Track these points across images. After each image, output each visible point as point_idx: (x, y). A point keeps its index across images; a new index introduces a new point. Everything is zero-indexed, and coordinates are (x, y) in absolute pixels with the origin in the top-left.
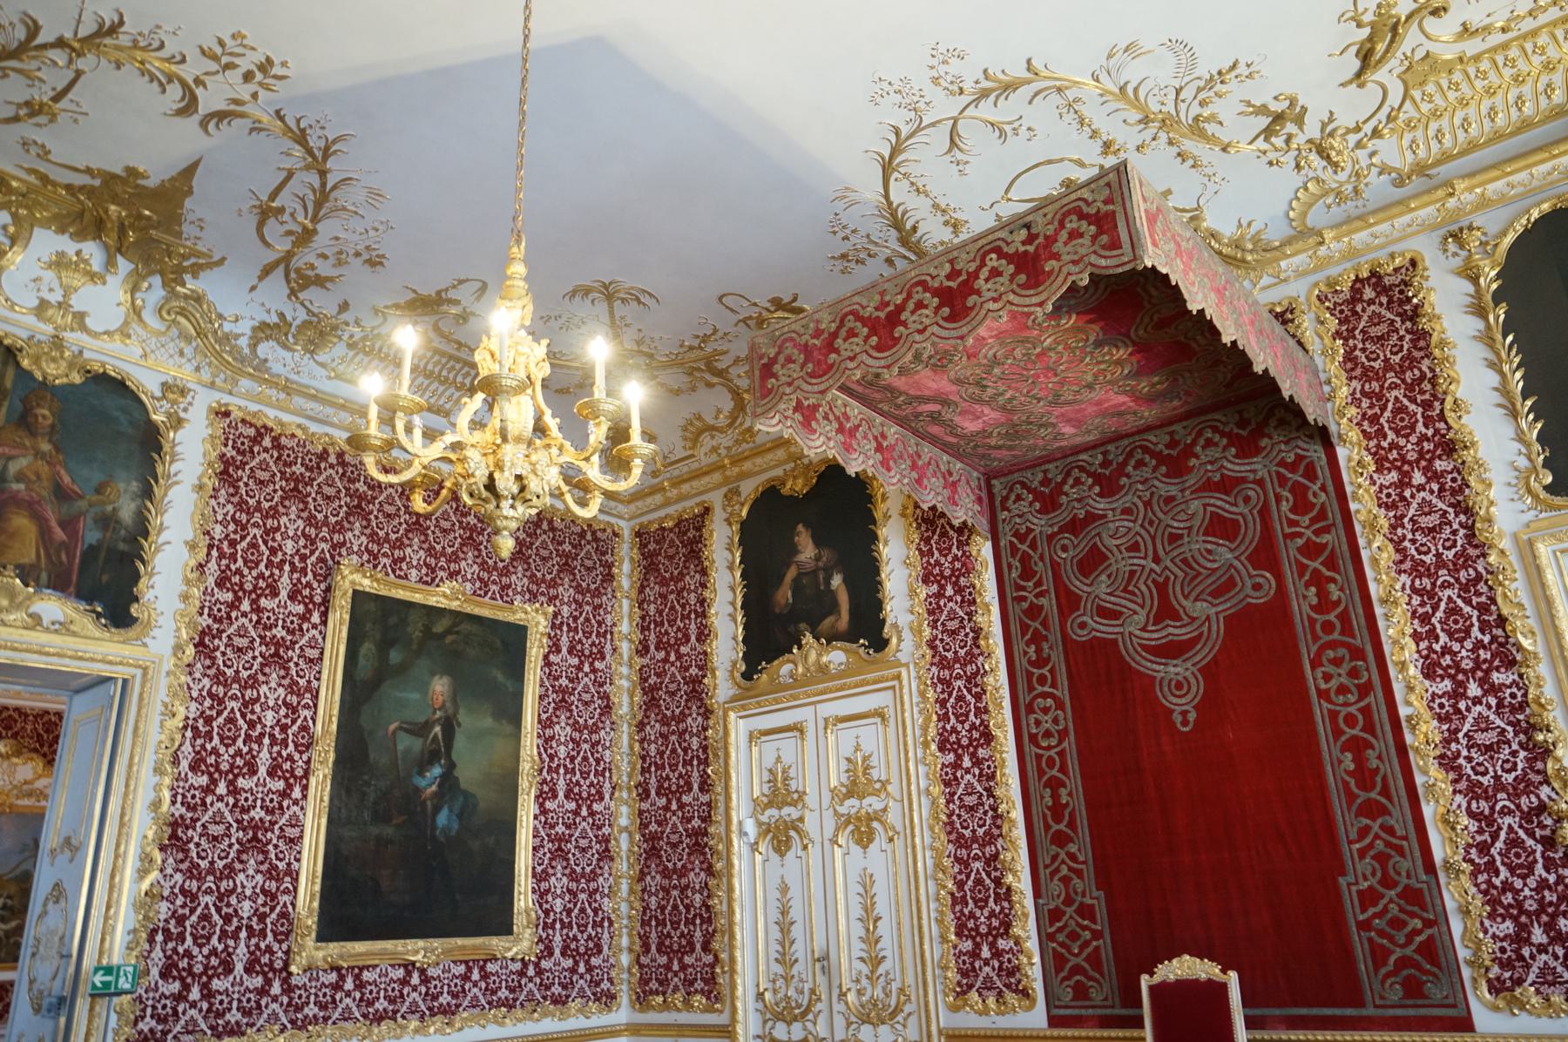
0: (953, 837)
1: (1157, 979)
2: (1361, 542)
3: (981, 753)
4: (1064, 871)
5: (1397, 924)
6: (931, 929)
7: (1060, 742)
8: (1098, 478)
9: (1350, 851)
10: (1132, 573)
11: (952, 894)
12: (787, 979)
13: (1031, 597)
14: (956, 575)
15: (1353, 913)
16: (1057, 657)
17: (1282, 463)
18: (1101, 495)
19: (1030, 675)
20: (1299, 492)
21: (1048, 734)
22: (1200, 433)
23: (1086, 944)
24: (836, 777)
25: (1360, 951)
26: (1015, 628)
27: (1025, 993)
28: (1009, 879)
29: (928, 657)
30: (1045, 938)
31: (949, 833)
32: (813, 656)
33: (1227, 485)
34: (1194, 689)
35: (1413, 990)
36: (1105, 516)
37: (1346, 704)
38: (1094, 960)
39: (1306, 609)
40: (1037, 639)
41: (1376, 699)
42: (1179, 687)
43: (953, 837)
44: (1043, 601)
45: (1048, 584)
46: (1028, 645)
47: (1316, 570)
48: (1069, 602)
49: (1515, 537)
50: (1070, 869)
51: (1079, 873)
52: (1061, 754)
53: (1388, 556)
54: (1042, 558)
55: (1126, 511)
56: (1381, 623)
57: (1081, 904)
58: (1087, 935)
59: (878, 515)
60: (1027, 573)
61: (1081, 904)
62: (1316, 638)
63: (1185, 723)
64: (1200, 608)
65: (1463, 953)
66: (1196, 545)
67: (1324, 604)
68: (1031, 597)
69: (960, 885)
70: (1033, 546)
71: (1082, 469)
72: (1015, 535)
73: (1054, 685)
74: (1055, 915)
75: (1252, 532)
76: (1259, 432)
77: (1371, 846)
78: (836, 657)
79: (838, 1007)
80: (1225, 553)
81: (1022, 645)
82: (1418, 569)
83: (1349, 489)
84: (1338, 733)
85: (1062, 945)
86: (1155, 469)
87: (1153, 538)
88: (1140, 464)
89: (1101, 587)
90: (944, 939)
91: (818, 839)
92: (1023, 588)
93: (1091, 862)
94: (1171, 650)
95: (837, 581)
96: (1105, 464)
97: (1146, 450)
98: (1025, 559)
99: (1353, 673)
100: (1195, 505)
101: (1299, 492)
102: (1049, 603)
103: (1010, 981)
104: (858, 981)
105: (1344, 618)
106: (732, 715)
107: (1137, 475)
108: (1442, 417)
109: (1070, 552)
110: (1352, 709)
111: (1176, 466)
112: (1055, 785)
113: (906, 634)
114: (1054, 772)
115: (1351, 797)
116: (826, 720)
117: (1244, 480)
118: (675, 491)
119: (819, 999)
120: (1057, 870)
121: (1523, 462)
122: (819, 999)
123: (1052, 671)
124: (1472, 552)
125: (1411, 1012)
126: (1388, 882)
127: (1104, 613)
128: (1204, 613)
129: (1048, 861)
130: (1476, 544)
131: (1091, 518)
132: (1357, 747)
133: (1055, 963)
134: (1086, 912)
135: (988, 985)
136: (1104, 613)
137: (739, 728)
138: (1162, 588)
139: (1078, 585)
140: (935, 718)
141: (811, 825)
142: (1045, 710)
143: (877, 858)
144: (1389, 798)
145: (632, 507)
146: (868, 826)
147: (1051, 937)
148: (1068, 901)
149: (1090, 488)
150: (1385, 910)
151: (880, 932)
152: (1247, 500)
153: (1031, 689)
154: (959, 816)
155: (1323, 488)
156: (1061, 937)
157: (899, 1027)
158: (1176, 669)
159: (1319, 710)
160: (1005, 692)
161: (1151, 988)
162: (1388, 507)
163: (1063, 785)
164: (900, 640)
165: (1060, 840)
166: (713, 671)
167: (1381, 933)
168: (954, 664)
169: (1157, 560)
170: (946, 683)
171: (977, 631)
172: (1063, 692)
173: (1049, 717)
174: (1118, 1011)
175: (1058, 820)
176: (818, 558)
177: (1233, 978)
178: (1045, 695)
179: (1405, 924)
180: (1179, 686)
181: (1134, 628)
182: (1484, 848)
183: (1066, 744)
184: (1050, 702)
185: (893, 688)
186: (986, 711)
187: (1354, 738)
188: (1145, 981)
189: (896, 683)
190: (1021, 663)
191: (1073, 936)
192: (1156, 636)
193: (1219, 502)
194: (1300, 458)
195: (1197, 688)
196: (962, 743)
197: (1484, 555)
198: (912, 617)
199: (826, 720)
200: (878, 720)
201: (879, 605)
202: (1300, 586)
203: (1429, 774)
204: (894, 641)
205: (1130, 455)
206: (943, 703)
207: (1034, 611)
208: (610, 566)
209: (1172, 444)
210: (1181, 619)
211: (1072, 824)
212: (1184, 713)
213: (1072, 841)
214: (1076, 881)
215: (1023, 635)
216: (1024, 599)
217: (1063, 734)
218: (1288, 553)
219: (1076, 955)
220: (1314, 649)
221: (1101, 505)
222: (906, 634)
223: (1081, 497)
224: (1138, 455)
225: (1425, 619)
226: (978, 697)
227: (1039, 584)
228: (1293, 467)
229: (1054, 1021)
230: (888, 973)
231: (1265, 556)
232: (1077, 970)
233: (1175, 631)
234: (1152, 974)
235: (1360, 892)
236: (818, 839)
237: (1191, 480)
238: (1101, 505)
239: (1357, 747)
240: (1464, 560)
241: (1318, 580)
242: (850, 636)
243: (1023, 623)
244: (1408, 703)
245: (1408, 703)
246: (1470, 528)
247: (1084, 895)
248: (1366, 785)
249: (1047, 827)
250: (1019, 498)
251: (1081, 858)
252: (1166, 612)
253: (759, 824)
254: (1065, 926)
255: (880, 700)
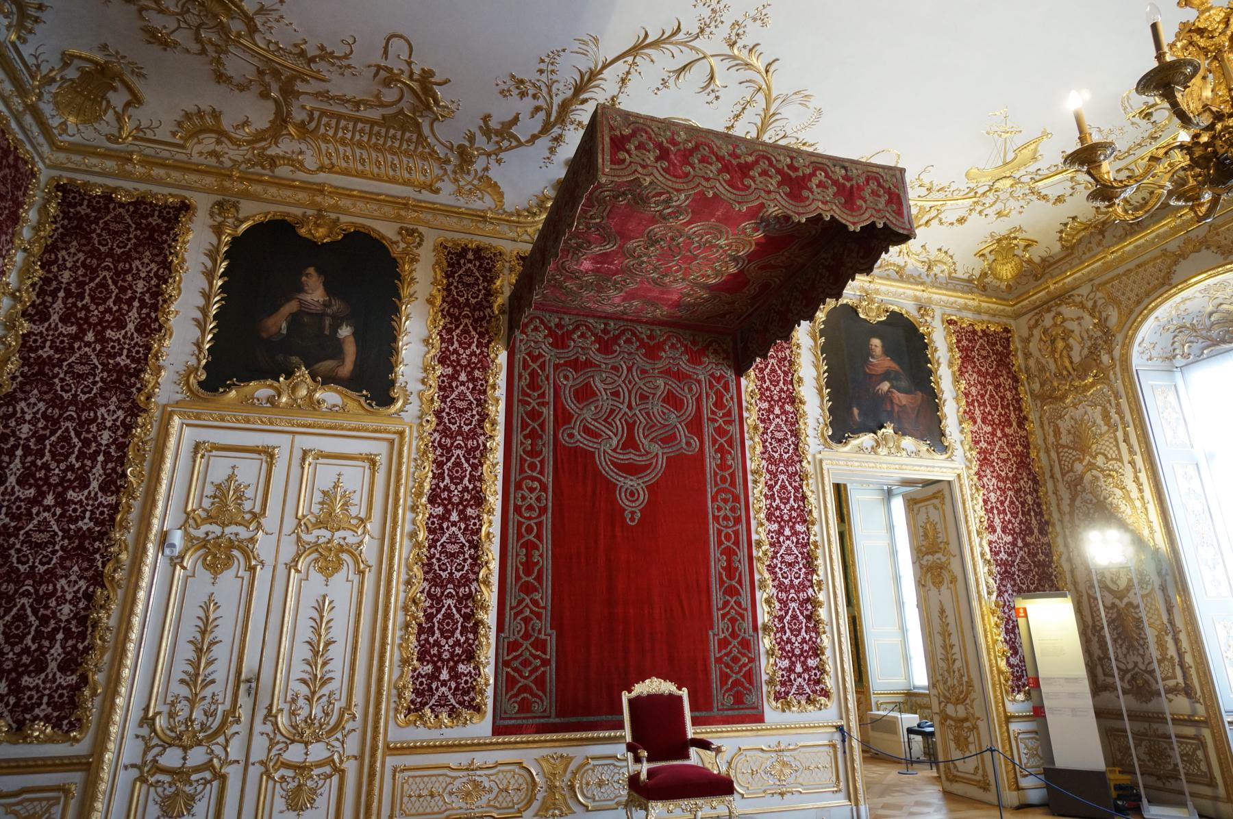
0: (430, 576)
1: (634, 694)
2: (746, 436)
3: (470, 512)
4: (527, 612)
5: (735, 660)
6: (393, 655)
7: (540, 515)
8: (598, 340)
9: (717, 615)
10: (612, 411)
11: (420, 625)
12: (192, 702)
13: (534, 404)
14: (470, 368)
15: (714, 652)
16: (548, 453)
17: (712, 375)
18: (599, 350)
19: (522, 460)
20: (719, 396)
21: (530, 508)
22: (668, 338)
23: (536, 669)
24: (309, 506)
25: (715, 675)
26: (516, 423)
27: (478, 709)
28: (481, 615)
29: (434, 425)
30: (501, 664)
31: (426, 573)
32: (303, 392)
33: (679, 376)
34: (642, 498)
35: (739, 699)
36: (596, 366)
37: (727, 527)
38: (541, 682)
39: (713, 465)
40: (533, 435)
41: (742, 527)
42: (633, 495)
43: (430, 576)
44: (545, 410)
45: (550, 397)
46: (525, 437)
47: (721, 445)
48: (563, 418)
49: (814, 456)
50: (532, 611)
51: (539, 616)
52: (539, 525)
53: (759, 449)
54: (547, 378)
55: (615, 368)
56: (750, 485)
57: (537, 638)
58: (538, 662)
59: (405, 292)
60: (533, 385)
61: (537, 638)
62: (716, 484)
63: (632, 519)
64: (655, 448)
65: (765, 677)
66: (656, 407)
67: (723, 466)
68: (534, 404)
69: (429, 617)
70: (542, 366)
71: (588, 328)
72: (529, 354)
73: (541, 472)
74: (514, 646)
75: (691, 408)
76: (703, 352)
77: (728, 613)
78: (330, 396)
79: (258, 727)
80: (673, 418)
81: (520, 437)
82: (770, 460)
83: (744, 404)
84: (720, 543)
85: (514, 669)
86: (638, 349)
87: (630, 393)
88: (628, 341)
89: (588, 414)
90: (405, 662)
91: (269, 561)
92: (529, 396)
93: (549, 608)
94: (632, 469)
95: (345, 332)
96: (605, 331)
97: (634, 334)
98: (533, 374)
99: (733, 509)
100: (660, 382)
101: (719, 396)
102: (548, 413)
103: (465, 700)
104: (294, 701)
105: (732, 475)
106: (176, 420)
107: (626, 348)
108: (791, 382)
109: (569, 382)
110: (730, 531)
111: (652, 352)
112: (530, 547)
113: (414, 399)
114: (531, 537)
115: (722, 582)
116: (305, 453)
117: (690, 377)
118: (142, 170)
119: (238, 721)
120: (521, 612)
121: (821, 420)
122: (238, 721)
123: (542, 462)
124: (796, 459)
125: (736, 712)
126: (734, 635)
127: (587, 430)
128: (656, 453)
129: (514, 604)
130: (798, 454)
131: (588, 364)
132: (729, 553)
133: (507, 683)
134: (540, 645)
135: (443, 702)
136: (587, 430)
137: (182, 435)
138: (631, 427)
139: (571, 405)
140: (430, 475)
141: (264, 546)
142: (531, 490)
143: (341, 587)
144: (741, 585)
145: (62, 157)
146: (337, 556)
147: (506, 664)
148: (526, 636)
149: (592, 343)
150: (731, 651)
151: (329, 655)
152: (690, 390)
153: (522, 471)
154: (439, 560)
155: (732, 398)
156: (516, 664)
157: (337, 744)
158: (631, 482)
159: (712, 528)
160: (500, 469)
161: (630, 701)
162: (763, 421)
163: (537, 548)
164: (405, 403)
165: (527, 589)
166: (159, 369)
167: (727, 666)
168: (455, 439)
169: (630, 407)
170: (447, 450)
171: (484, 416)
172: (548, 479)
173: (534, 496)
174: (554, 720)
175: (528, 572)
176: (326, 305)
177: (684, 693)
178: (533, 479)
179: (521, 663)
180: (632, 494)
181: (607, 450)
182: (781, 619)
183: (544, 518)
184: (536, 484)
185: (392, 442)
186: (481, 479)
187: (729, 548)
188: (625, 696)
189: (395, 436)
190: (517, 450)
191: (526, 663)
192: (623, 458)
193: (673, 384)
194: (722, 377)
195: (643, 497)
196: (452, 500)
197: (801, 461)
198: (422, 387)
199: (305, 453)
200: (367, 464)
201: (391, 368)
202: (712, 451)
203: (762, 573)
204: (400, 404)
205: (623, 333)
206: (440, 465)
207: (535, 415)
208: (19, 205)
209: (651, 337)
210: (639, 450)
211: (539, 578)
212: (633, 513)
213: (537, 590)
214: (536, 621)
215: (522, 430)
216: (529, 404)
217: (543, 510)
218: (708, 430)
219: (526, 678)
220: (715, 490)
221: (598, 358)
222: (414, 399)
223: (584, 346)
224: (628, 335)
225: (771, 488)
226: (474, 467)
227: (543, 395)
228: (718, 380)
229: (497, 731)
230: (331, 693)
231: (695, 427)
232: (525, 689)
233: (632, 457)
234: (630, 692)
235: (719, 641)
236: (269, 561)
237: (660, 364)
238: (598, 358)
239: (729, 553)
240: (790, 462)
241: (721, 450)
242: (352, 383)
243: (524, 421)
244: (757, 532)
245: (757, 532)
246: (797, 445)
247: (540, 632)
248: (731, 578)
249: (518, 578)
250: (536, 329)
251: (542, 604)
252: (630, 443)
253: (188, 537)
254: (521, 655)
255: (378, 448)
